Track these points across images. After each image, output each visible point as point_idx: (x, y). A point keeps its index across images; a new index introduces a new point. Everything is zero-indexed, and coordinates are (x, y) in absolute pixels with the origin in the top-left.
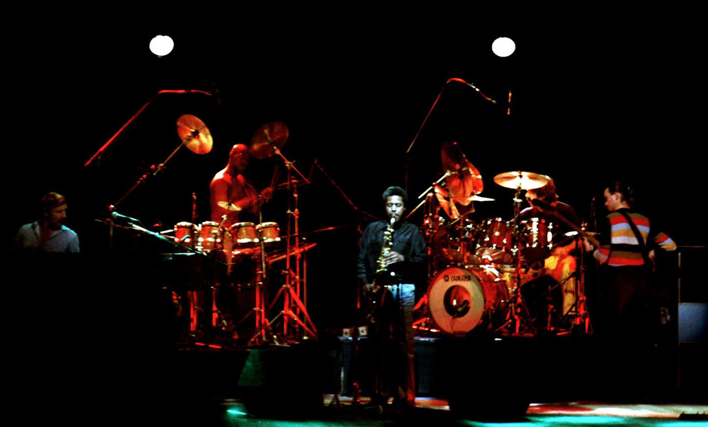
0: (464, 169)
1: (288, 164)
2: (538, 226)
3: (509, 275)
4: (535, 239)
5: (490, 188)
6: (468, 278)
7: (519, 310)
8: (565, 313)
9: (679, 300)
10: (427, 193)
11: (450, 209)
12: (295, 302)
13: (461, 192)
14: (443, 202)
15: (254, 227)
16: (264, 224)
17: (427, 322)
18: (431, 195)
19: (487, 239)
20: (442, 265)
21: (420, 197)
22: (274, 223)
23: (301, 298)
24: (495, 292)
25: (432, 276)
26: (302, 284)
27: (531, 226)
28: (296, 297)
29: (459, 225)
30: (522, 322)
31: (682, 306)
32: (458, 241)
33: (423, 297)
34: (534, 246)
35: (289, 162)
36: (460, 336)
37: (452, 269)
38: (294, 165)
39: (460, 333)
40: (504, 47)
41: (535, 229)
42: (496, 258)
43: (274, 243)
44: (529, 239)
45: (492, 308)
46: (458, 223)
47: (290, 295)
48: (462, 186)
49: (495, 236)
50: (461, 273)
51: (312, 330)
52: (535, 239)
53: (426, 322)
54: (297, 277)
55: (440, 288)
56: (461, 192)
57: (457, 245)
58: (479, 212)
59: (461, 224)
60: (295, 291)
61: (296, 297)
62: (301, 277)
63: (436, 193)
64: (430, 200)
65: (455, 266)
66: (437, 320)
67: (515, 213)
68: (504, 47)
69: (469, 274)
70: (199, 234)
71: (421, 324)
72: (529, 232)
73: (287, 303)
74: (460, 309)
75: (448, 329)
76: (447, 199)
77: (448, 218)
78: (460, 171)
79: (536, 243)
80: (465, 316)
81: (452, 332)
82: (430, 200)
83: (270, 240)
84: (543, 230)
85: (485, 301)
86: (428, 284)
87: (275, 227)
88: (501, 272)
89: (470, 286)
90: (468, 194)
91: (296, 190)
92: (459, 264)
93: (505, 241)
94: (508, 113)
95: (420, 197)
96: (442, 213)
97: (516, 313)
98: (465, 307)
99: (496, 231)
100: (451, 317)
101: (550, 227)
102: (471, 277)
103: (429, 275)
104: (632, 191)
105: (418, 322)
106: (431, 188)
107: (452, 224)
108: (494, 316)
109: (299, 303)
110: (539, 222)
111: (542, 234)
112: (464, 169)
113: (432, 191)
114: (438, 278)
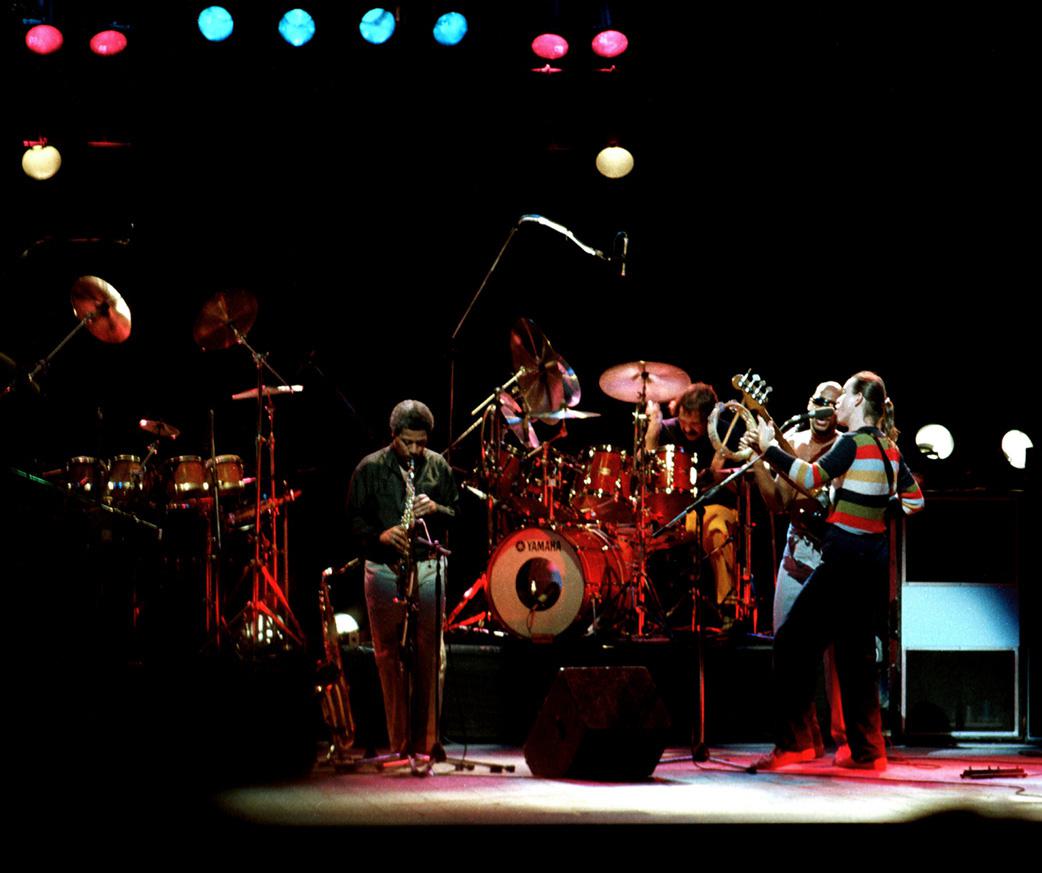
0: (549, 364)
1: (257, 357)
2: (673, 459)
3: (626, 541)
4: (670, 480)
5: (593, 397)
6: (556, 546)
7: (642, 598)
8: (720, 601)
9: (904, 578)
10: (486, 404)
11: (526, 432)
12: (270, 588)
13: (543, 402)
14: (513, 419)
15: (203, 464)
16: (220, 459)
17: (489, 619)
18: (493, 408)
19: (588, 481)
20: (513, 520)
21: (474, 412)
22: (235, 457)
23: (280, 581)
24: (603, 566)
25: (494, 542)
26: (281, 557)
27: (663, 457)
28: (271, 580)
29: (541, 458)
30: (646, 618)
31: (908, 588)
32: (539, 484)
33: (480, 577)
34: (669, 491)
35: (259, 356)
36: (544, 641)
37: (530, 531)
38: (267, 360)
39: (545, 637)
40: (615, 161)
41: (669, 464)
42: (603, 512)
43: (235, 490)
44: (658, 480)
45: (597, 595)
46: (540, 454)
47: (262, 577)
48: (545, 391)
49: (601, 475)
50: (541, 537)
51: (297, 635)
52: (670, 480)
53: (486, 620)
54: (275, 546)
55: (508, 564)
56: (543, 402)
57: (536, 492)
58: (573, 439)
59: (545, 457)
60: (271, 572)
61: (271, 580)
62: (280, 546)
63: (502, 405)
64: (492, 417)
65: (536, 525)
66: (504, 615)
67: (636, 437)
68: (615, 161)
69: (557, 538)
70: (108, 477)
71: (477, 622)
72: (658, 468)
73: (256, 590)
74: (543, 598)
75: (522, 630)
76: (521, 415)
77: (524, 448)
78: (542, 366)
79: (672, 487)
80: (557, 605)
81: (530, 636)
82: (492, 417)
83: (227, 485)
84: (682, 463)
85: (585, 584)
86: (489, 557)
87: (237, 463)
88: (612, 538)
89: (560, 563)
90: (556, 407)
91: (108, 492)
92: (542, 521)
93: (618, 483)
94: (623, 274)
95: (474, 412)
96: (512, 438)
97: (639, 603)
98: (552, 591)
99: (603, 466)
100: (528, 610)
101: (695, 460)
102: (562, 543)
103: (491, 541)
104: (589, 467)
105: (472, 620)
106: (493, 396)
107: (529, 455)
108: (606, 607)
109: (277, 588)
110: (677, 451)
111: (682, 471)
112: (549, 364)
113: (495, 402)
114: (505, 547)
